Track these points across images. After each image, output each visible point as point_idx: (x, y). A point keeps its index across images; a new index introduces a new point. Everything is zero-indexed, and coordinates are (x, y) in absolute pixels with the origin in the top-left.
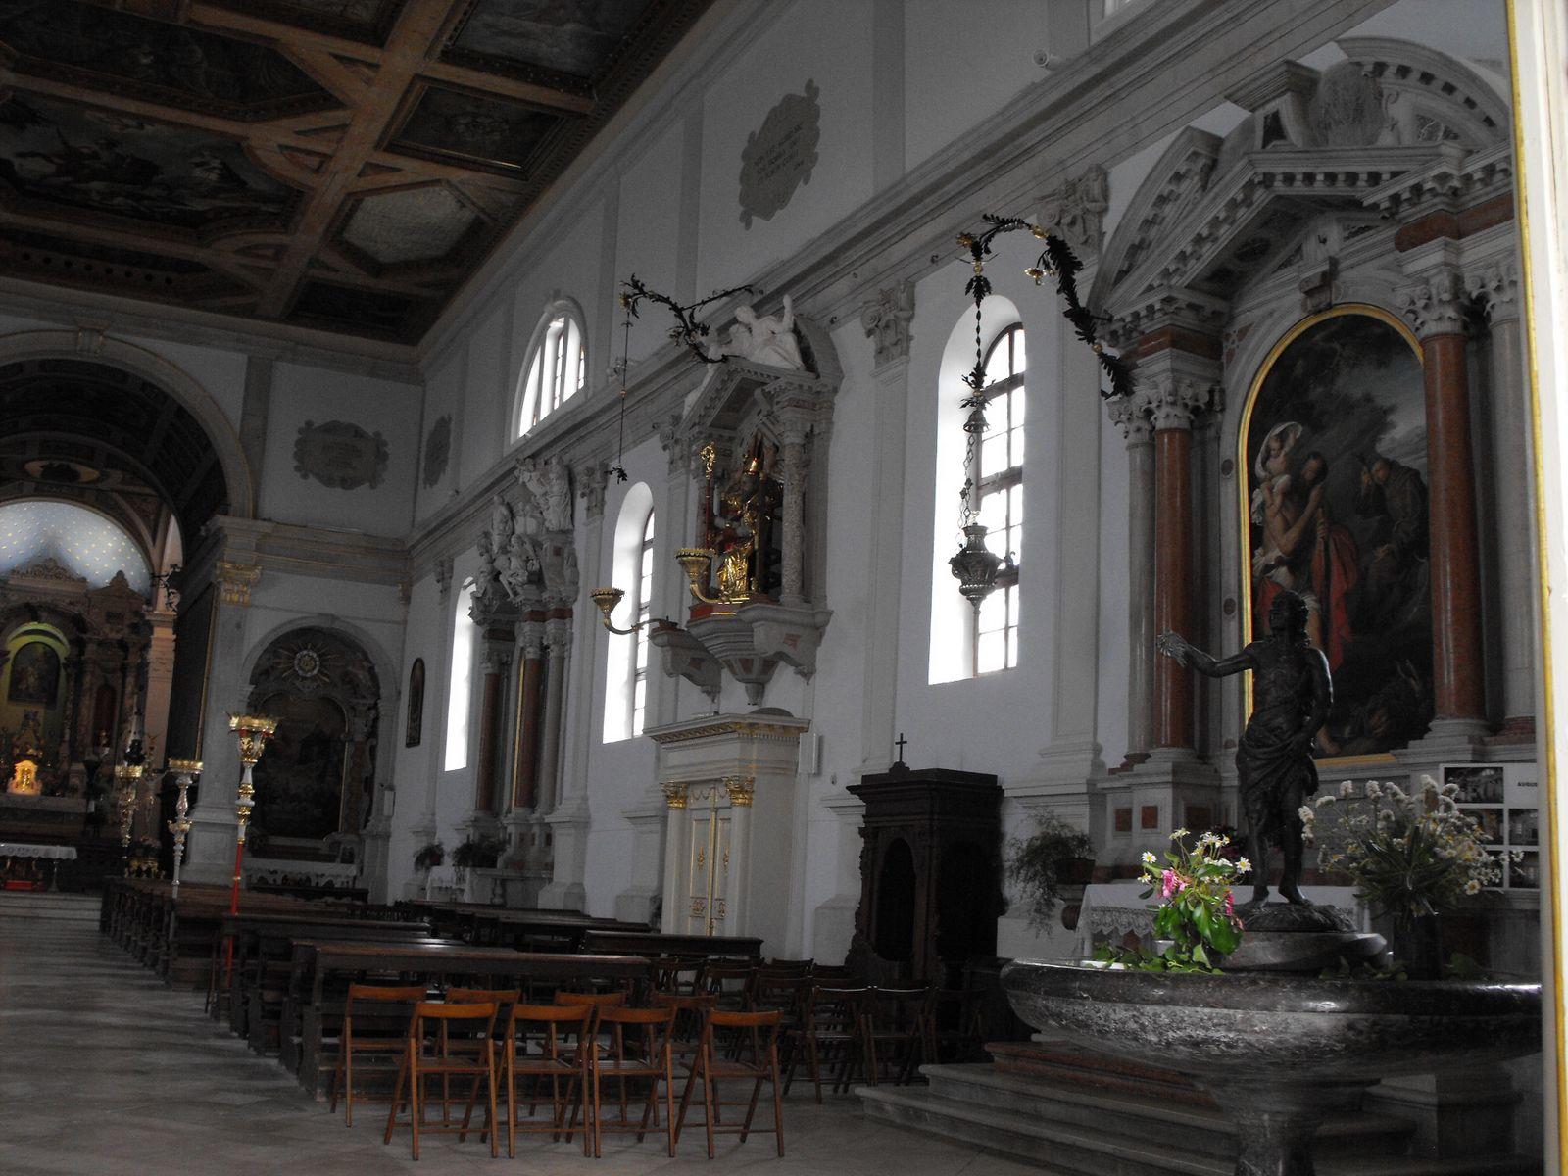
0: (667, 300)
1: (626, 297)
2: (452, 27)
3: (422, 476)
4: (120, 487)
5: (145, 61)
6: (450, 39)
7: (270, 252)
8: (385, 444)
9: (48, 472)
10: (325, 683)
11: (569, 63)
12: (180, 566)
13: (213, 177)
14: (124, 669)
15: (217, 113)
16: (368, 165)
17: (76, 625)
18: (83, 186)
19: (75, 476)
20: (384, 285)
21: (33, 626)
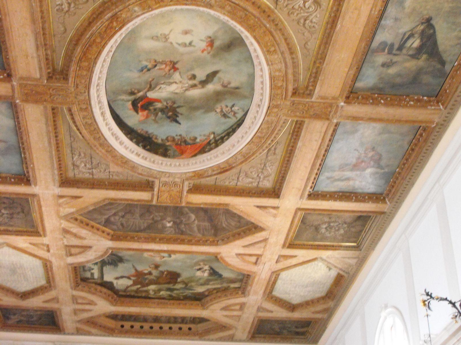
0: (446, 299)
1: (424, 302)
2: (311, 182)
5: (169, 225)
6: (311, 187)
7: (238, 307)
13: (206, 274)
15: (205, 243)
18: (145, 289)
20: (297, 315)
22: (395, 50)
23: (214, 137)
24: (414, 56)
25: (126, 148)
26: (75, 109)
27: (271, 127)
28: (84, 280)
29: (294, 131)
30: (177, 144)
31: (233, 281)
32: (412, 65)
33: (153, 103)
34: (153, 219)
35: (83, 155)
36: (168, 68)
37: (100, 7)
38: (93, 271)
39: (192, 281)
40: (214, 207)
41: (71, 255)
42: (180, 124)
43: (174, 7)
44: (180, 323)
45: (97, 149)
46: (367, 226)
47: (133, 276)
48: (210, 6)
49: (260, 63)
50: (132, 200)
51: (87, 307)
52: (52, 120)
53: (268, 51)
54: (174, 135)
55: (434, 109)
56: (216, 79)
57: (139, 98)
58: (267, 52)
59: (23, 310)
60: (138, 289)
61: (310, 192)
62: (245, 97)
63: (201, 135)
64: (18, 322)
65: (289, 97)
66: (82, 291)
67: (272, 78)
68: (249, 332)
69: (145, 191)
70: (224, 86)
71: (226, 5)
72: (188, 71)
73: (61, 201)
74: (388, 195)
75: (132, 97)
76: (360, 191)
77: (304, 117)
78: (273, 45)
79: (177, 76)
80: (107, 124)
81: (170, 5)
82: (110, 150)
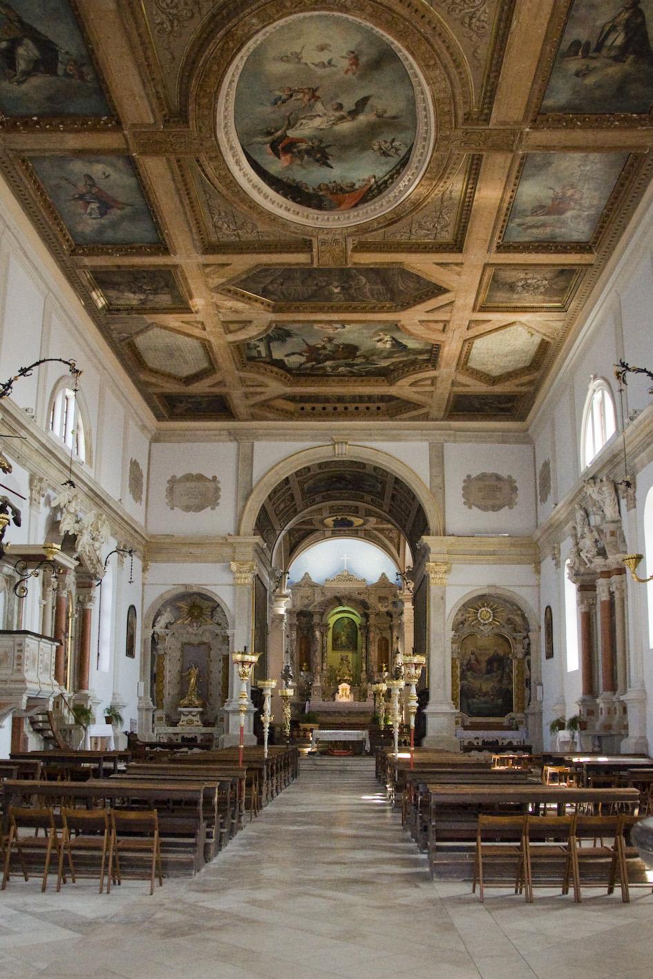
3: (539, 497)
4: (376, 526)
5: (336, 291)
6: (500, 238)
7: (429, 382)
8: (515, 482)
9: (337, 523)
10: (497, 626)
11: (576, 236)
12: (412, 566)
13: (388, 346)
14: (391, 628)
15: (381, 310)
16: (470, 322)
17: (363, 606)
18: (319, 365)
19: (350, 524)
20: (499, 389)
21: (341, 608)
22: (591, 51)
23: (376, 182)
24: (618, 59)
25: (273, 203)
26: (203, 158)
27: (442, 165)
28: (251, 359)
29: (471, 168)
30: (332, 193)
31: (420, 352)
32: (614, 71)
33: (295, 143)
34: (317, 285)
35: (223, 214)
36: (307, 97)
37: (210, 22)
38: (259, 349)
39: (372, 355)
40: (385, 266)
41: (230, 332)
42: (332, 167)
43: (302, 15)
44: (367, 402)
45: (238, 205)
46: (573, 282)
47: (305, 352)
48: (344, 9)
49: (420, 84)
50: (290, 264)
51: (259, 389)
52: (179, 174)
53: (428, 66)
54: (326, 182)
55: (647, 130)
56: (367, 108)
57: (278, 138)
58: (426, 67)
59: (190, 397)
60: (313, 366)
61: (498, 243)
62: (407, 128)
63: (359, 180)
64: (186, 411)
65: (460, 126)
66: (250, 372)
67: (436, 102)
68: (446, 410)
69: (303, 252)
70: (379, 116)
71: (366, 6)
72: (332, 99)
73: (208, 270)
74: (595, 243)
75: (269, 139)
76: (559, 239)
77: (481, 150)
78: (431, 58)
79: (319, 107)
80: (245, 175)
81: (295, 13)
82: (254, 206)
